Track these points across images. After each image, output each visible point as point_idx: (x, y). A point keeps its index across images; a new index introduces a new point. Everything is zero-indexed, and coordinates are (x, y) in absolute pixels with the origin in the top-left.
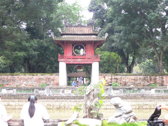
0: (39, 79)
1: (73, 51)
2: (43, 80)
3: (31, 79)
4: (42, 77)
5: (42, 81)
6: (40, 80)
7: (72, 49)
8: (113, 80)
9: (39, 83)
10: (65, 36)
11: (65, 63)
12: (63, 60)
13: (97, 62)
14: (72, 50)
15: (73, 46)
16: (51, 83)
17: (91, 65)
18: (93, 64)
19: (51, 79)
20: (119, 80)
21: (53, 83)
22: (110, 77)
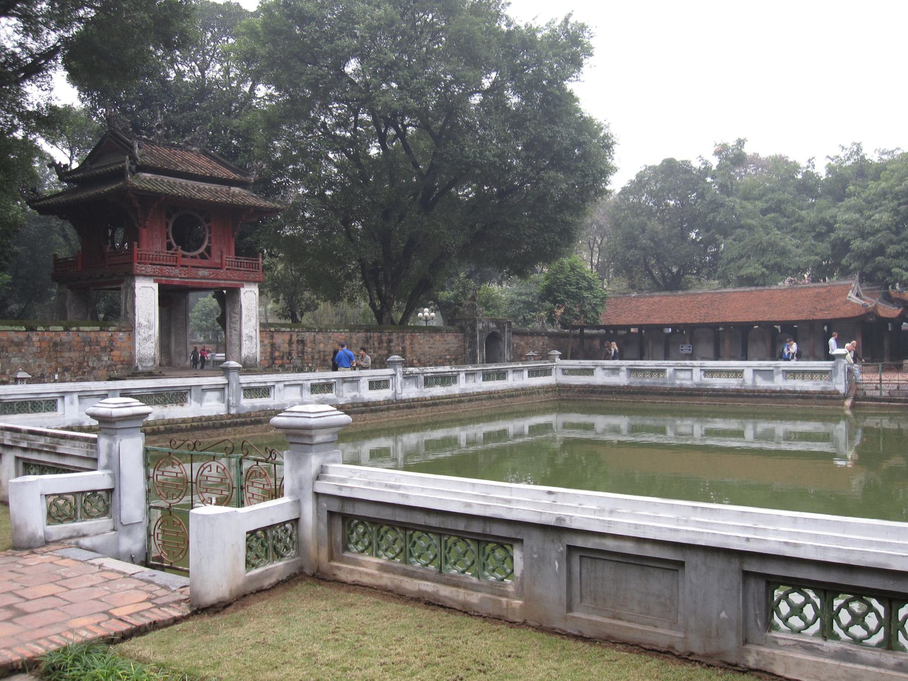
0: (55, 344)
1: (168, 238)
2: (70, 350)
3: (19, 344)
4: (64, 337)
5: (66, 355)
6: (59, 348)
7: (167, 227)
8: (294, 346)
9: (53, 363)
10: (148, 175)
11: (155, 282)
12: (149, 269)
13: (255, 282)
14: (167, 234)
15: (169, 216)
16: (99, 359)
17: (234, 292)
18: (243, 290)
19: (102, 344)
20: (309, 345)
21: (109, 362)
22: (287, 337)
